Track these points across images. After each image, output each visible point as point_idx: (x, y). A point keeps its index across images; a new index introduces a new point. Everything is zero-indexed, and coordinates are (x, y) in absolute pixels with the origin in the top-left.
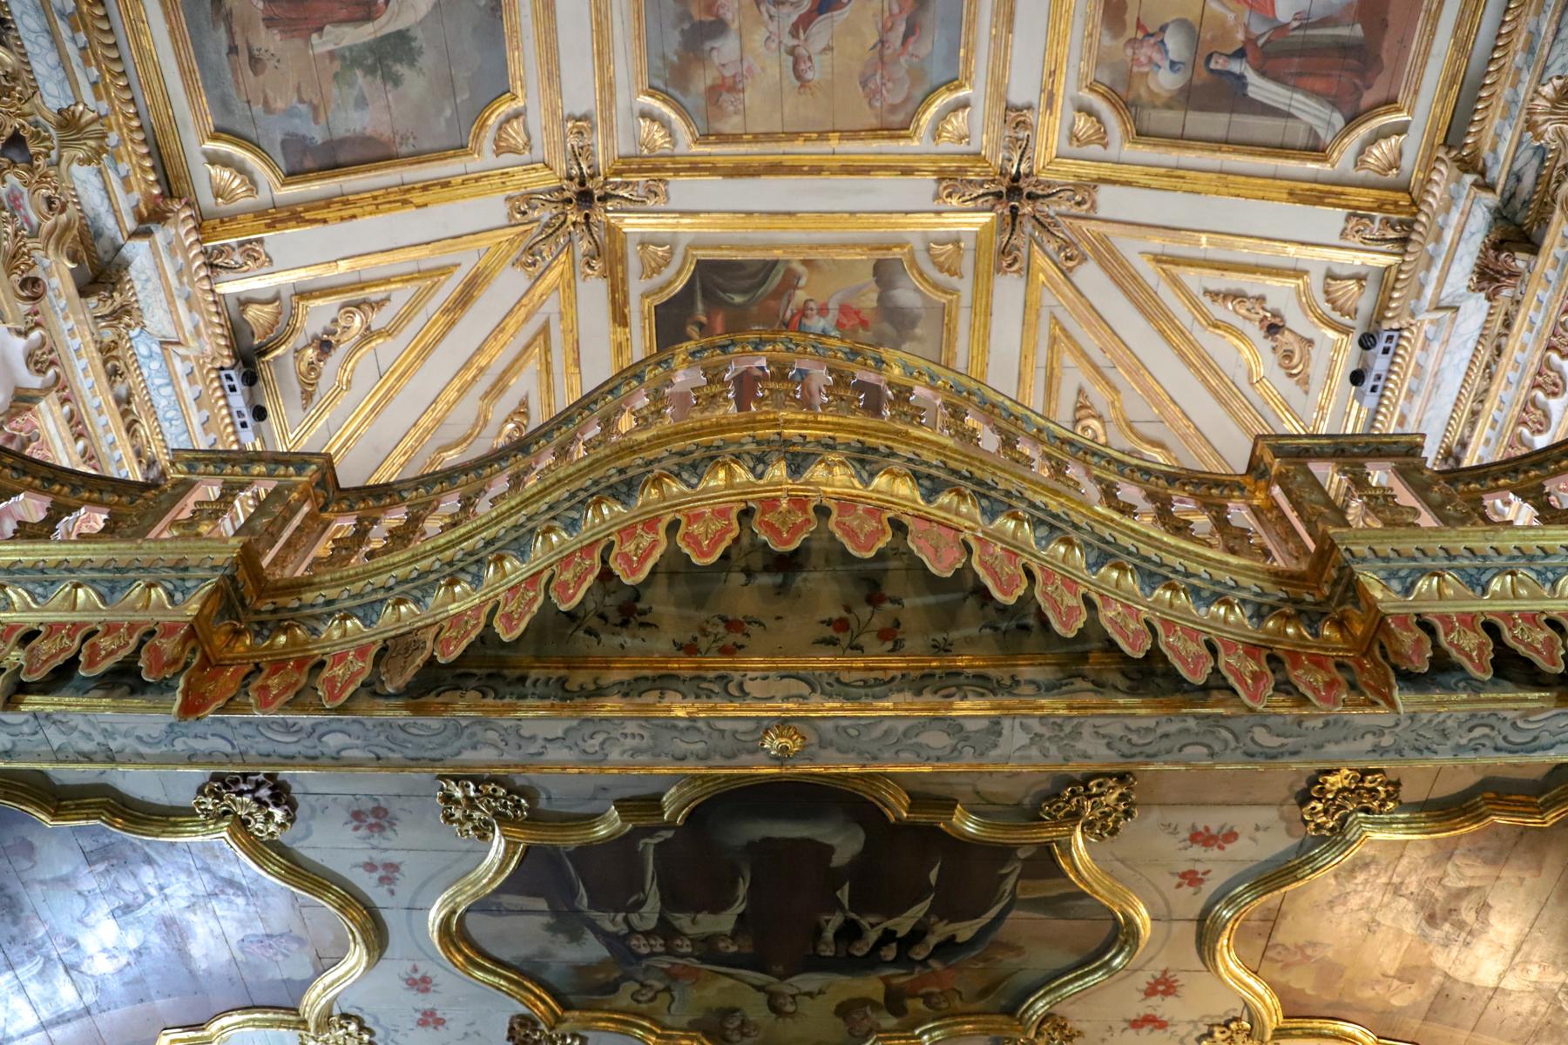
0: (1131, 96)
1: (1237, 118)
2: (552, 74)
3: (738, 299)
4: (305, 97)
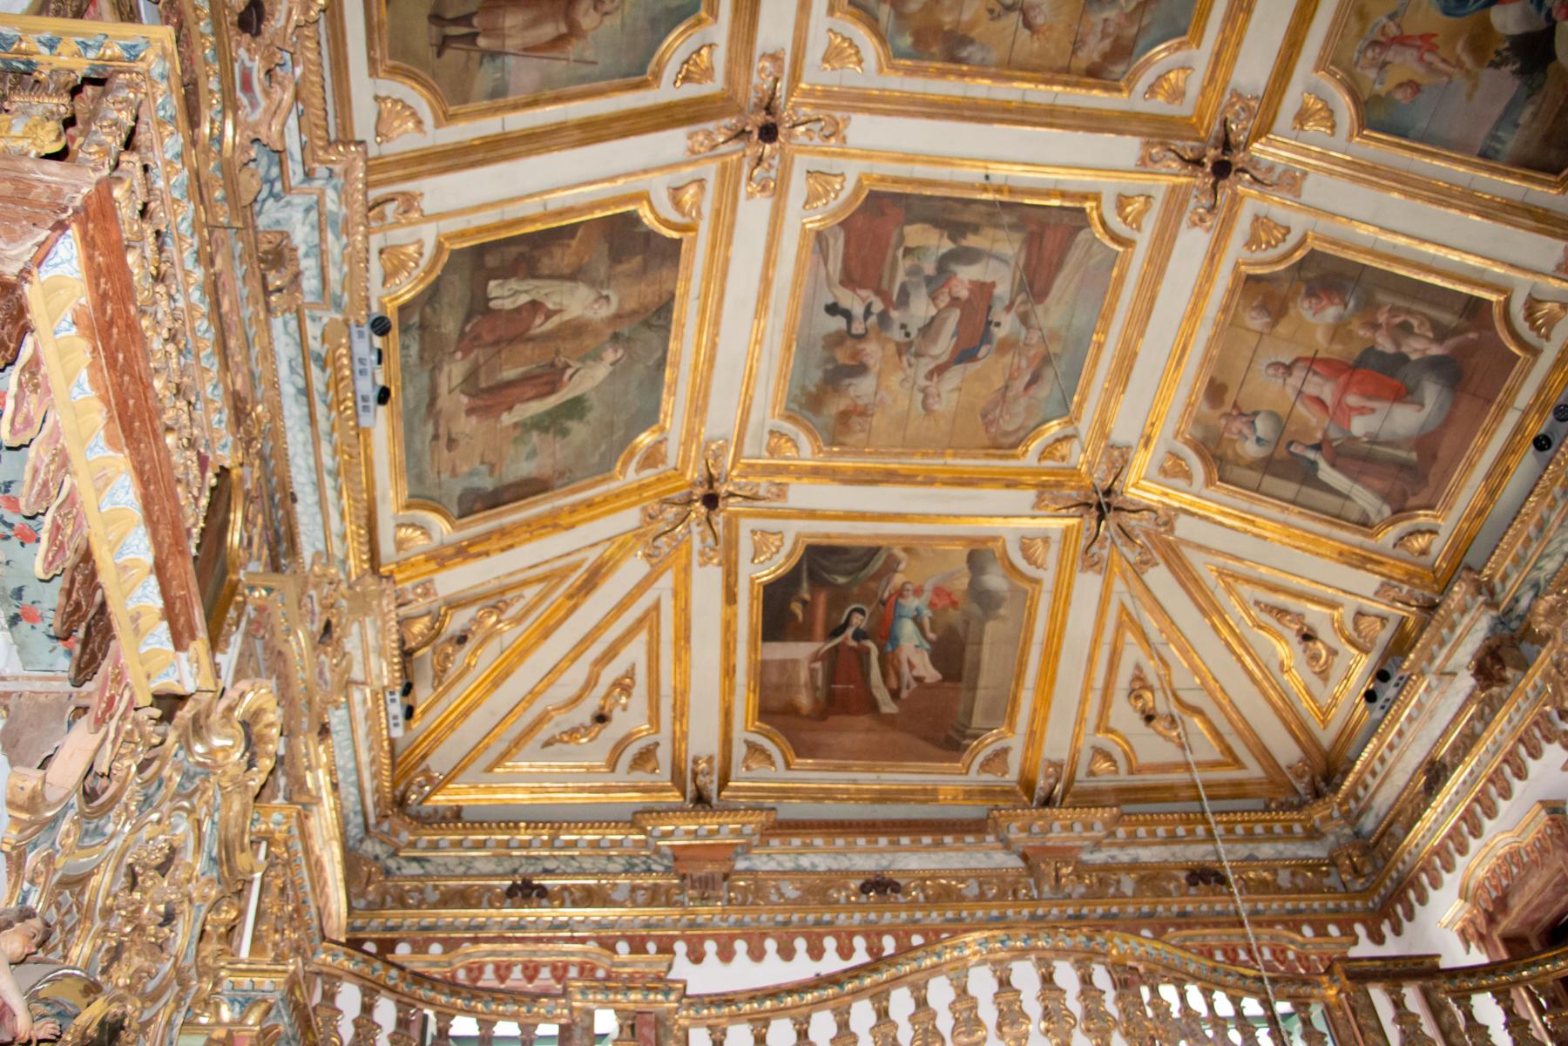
0: (1218, 452)
1: (1305, 489)
2: (699, 407)
3: (841, 580)
4: (487, 459)
